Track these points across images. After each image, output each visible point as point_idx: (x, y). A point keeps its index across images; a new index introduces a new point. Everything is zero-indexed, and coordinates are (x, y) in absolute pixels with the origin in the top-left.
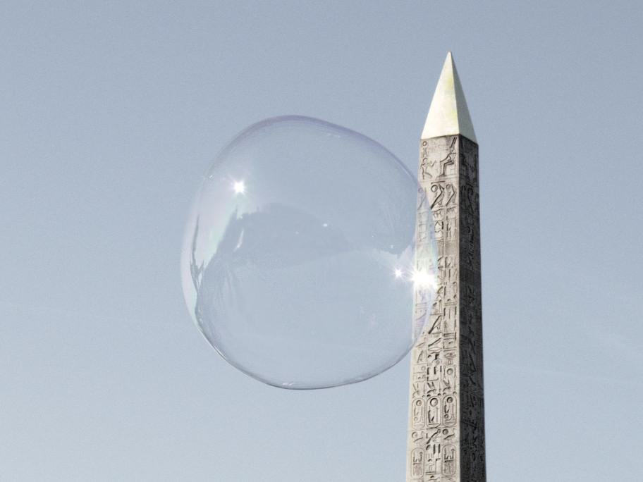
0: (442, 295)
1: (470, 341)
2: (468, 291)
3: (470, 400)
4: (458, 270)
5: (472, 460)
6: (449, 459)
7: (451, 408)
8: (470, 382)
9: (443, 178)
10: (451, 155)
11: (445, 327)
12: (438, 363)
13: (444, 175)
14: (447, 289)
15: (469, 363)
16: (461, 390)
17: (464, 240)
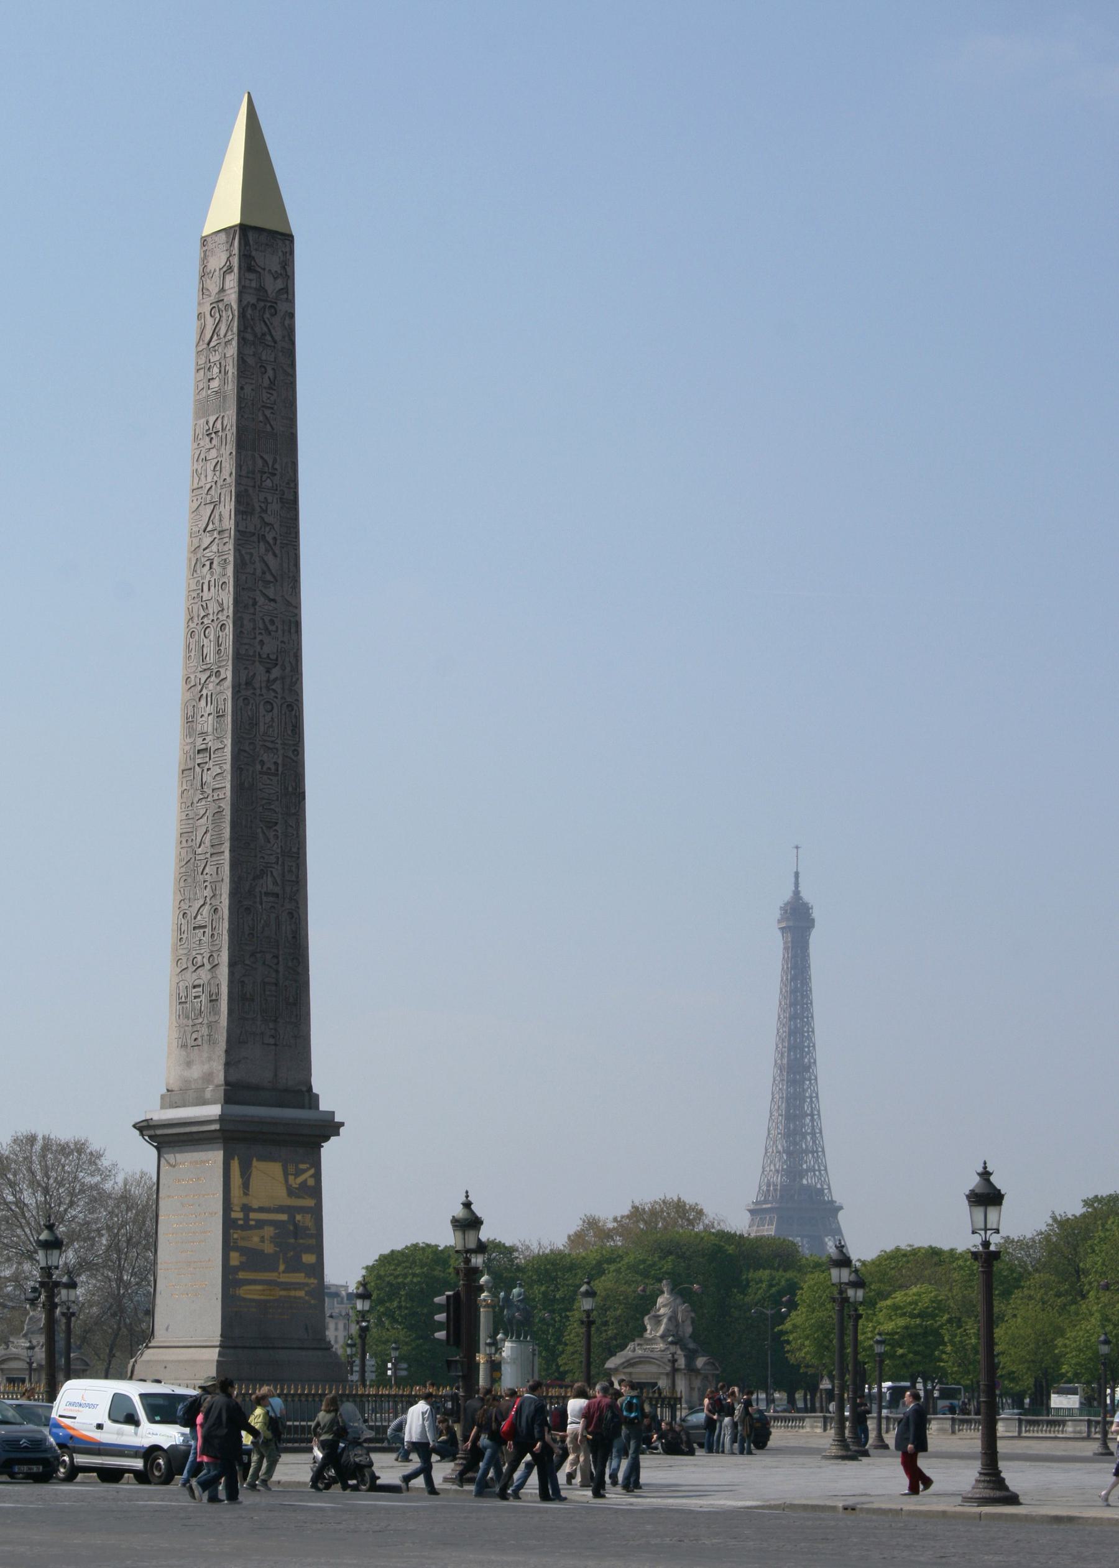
0: (218, 473)
2: (260, 462)
3: (261, 626)
4: (235, 433)
6: (221, 714)
7: (224, 639)
8: (261, 600)
9: (222, 294)
10: (231, 259)
11: (220, 520)
12: (212, 574)
13: (222, 290)
14: (223, 465)
15: (259, 572)
16: (235, 612)
17: (248, 389)
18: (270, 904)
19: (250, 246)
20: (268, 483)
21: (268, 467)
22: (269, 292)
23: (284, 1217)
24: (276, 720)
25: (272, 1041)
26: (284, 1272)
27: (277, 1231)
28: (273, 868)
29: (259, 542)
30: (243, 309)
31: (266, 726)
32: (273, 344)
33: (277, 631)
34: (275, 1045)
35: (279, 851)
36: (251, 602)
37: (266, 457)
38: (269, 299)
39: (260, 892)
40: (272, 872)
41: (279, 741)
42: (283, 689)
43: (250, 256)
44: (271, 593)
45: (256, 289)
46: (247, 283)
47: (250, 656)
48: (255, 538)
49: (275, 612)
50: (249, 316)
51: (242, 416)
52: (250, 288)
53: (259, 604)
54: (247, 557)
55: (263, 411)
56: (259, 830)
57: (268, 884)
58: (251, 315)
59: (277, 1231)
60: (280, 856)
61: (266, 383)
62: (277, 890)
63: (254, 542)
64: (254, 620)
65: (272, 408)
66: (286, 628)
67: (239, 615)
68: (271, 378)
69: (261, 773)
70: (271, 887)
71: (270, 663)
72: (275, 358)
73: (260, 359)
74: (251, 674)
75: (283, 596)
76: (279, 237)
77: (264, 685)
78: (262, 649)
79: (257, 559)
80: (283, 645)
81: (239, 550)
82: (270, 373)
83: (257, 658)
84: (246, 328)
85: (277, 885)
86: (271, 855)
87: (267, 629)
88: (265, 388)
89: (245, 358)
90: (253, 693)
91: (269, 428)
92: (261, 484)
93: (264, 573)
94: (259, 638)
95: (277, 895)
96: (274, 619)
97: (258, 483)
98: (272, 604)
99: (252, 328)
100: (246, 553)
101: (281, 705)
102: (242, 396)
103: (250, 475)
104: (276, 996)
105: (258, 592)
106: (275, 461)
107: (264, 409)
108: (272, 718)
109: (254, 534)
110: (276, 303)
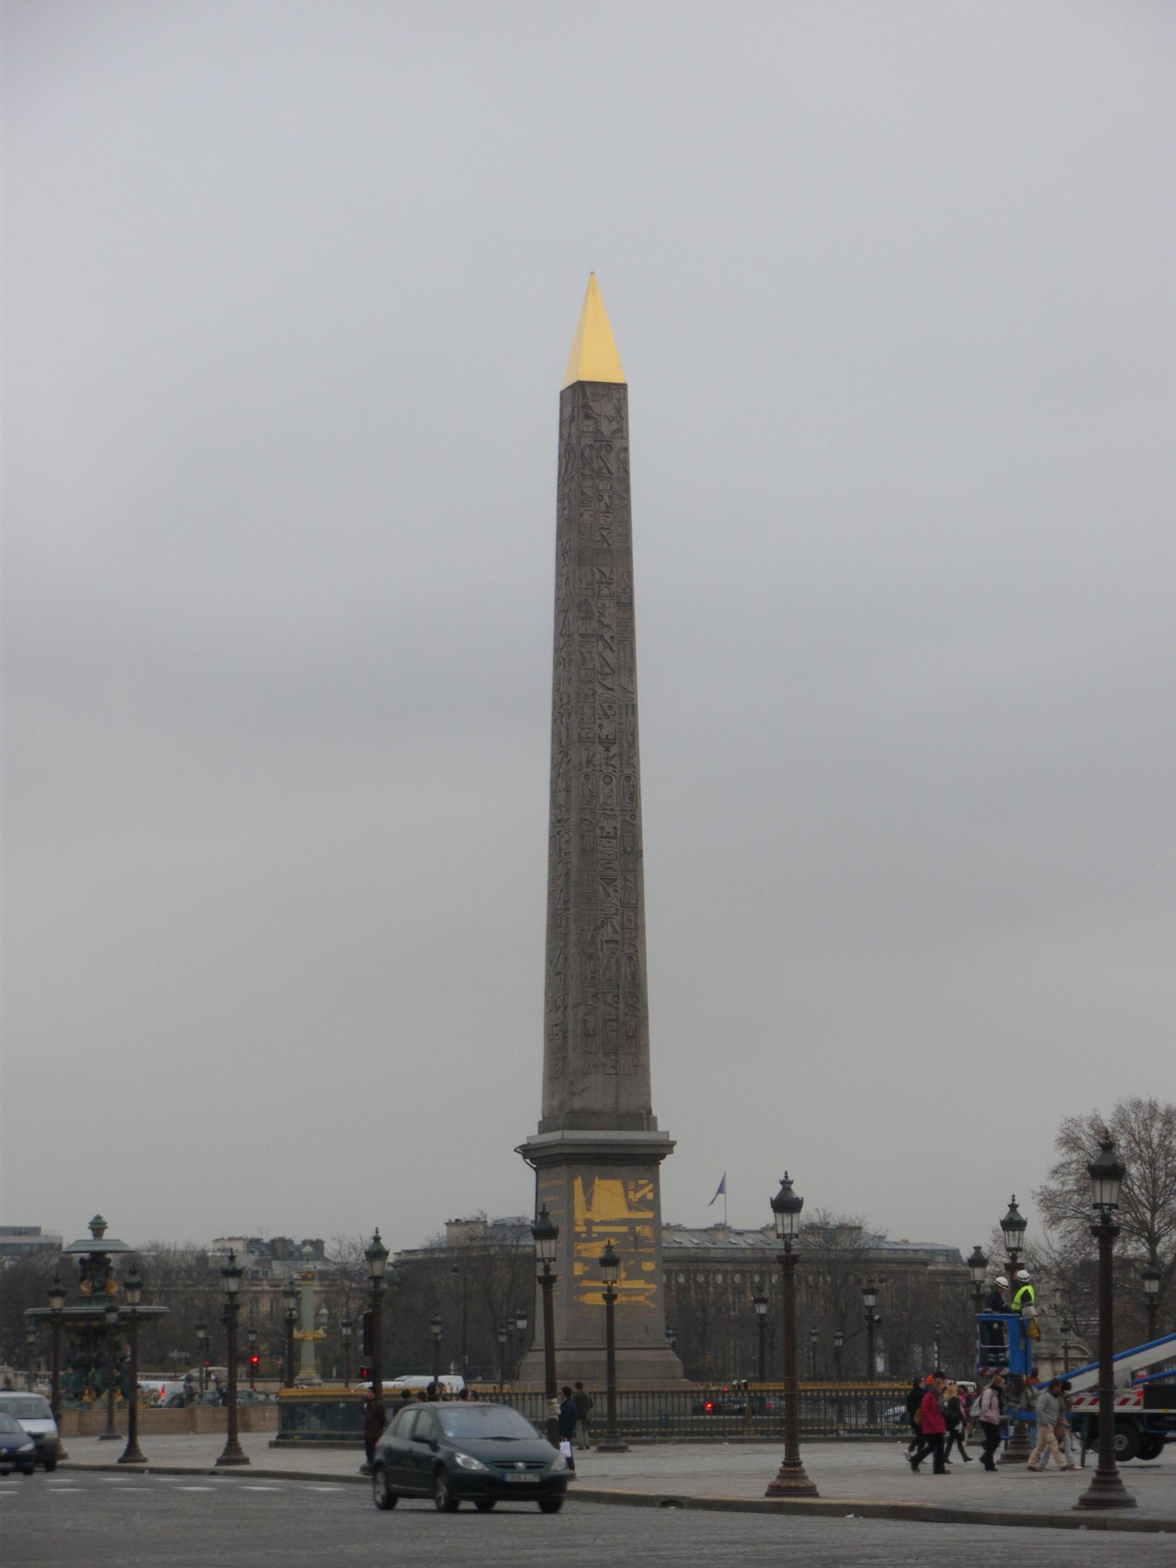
1: (602, 638)
2: (598, 575)
5: (602, 784)
8: (600, 690)
15: (598, 665)
17: (586, 516)
18: (611, 951)
19: (588, 398)
20: (606, 591)
21: (605, 577)
22: (605, 433)
23: (624, 1229)
24: (615, 791)
25: (613, 1071)
26: (624, 1280)
27: (619, 1242)
28: (612, 918)
29: (597, 641)
30: (582, 451)
31: (606, 796)
32: (609, 476)
33: (615, 714)
34: (616, 1074)
35: (618, 903)
36: (591, 692)
37: (603, 570)
38: (605, 439)
39: (601, 940)
40: (611, 922)
41: (618, 809)
42: (621, 764)
43: (588, 406)
44: (608, 683)
45: (593, 432)
46: (585, 429)
47: (590, 738)
48: (594, 639)
49: (613, 699)
50: (587, 456)
51: (582, 539)
52: (588, 432)
53: (598, 694)
54: (587, 656)
55: (600, 532)
56: (600, 887)
57: (608, 933)
58: (588, 454)
59: (619, 1242)
60: (619, 907)
61: (603, 508)
62: (617, 937)
63: (594, 642)
64: (594, 708)
65: (609, 529)
66: (624, 712)
67: (580, 705)
68: (609, 505)
69: (601, 837)
70: (611, 936)
71: (607, 743)
72: (611, 487)
73: (598, 489)
74: (591, 753)
75: (620, 685)
76: (614, 387)
77: (603, 761)
78: (601, 731)
79: (596, 656)
80: (621, 726)
81: (580, 650)
82: (606, 499)
83: (597, 740)
84: (584, 465)
85: (618, 933)
86: (612, 907)
87: (607, 716)
88: (602, 513)
89: (584, 490)
90: (594, 770)
91: (606, 546)
92: (599, 592)
93: (602, 667)
94: (598, 722)
95: (617, 942)
96: (613, 705)
97: (596, 592)
98: (610, 692)
99: (590, 465)
100: (586, 652)
101: (620, 777)
102: (582, 522)
103: (589, 587)
104: (616, 1031)
105: (597, 685)
106: (612, 571)
107: (601, 530)
108: (611, 789)
109: (593, 635)
110: (612, 442)
